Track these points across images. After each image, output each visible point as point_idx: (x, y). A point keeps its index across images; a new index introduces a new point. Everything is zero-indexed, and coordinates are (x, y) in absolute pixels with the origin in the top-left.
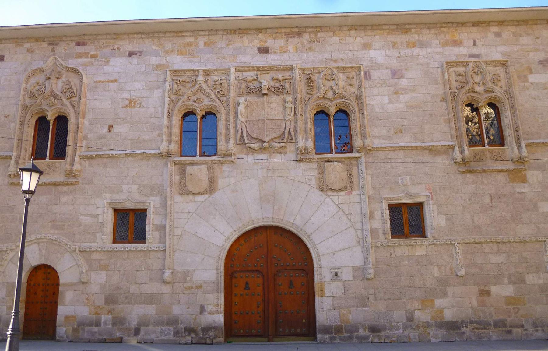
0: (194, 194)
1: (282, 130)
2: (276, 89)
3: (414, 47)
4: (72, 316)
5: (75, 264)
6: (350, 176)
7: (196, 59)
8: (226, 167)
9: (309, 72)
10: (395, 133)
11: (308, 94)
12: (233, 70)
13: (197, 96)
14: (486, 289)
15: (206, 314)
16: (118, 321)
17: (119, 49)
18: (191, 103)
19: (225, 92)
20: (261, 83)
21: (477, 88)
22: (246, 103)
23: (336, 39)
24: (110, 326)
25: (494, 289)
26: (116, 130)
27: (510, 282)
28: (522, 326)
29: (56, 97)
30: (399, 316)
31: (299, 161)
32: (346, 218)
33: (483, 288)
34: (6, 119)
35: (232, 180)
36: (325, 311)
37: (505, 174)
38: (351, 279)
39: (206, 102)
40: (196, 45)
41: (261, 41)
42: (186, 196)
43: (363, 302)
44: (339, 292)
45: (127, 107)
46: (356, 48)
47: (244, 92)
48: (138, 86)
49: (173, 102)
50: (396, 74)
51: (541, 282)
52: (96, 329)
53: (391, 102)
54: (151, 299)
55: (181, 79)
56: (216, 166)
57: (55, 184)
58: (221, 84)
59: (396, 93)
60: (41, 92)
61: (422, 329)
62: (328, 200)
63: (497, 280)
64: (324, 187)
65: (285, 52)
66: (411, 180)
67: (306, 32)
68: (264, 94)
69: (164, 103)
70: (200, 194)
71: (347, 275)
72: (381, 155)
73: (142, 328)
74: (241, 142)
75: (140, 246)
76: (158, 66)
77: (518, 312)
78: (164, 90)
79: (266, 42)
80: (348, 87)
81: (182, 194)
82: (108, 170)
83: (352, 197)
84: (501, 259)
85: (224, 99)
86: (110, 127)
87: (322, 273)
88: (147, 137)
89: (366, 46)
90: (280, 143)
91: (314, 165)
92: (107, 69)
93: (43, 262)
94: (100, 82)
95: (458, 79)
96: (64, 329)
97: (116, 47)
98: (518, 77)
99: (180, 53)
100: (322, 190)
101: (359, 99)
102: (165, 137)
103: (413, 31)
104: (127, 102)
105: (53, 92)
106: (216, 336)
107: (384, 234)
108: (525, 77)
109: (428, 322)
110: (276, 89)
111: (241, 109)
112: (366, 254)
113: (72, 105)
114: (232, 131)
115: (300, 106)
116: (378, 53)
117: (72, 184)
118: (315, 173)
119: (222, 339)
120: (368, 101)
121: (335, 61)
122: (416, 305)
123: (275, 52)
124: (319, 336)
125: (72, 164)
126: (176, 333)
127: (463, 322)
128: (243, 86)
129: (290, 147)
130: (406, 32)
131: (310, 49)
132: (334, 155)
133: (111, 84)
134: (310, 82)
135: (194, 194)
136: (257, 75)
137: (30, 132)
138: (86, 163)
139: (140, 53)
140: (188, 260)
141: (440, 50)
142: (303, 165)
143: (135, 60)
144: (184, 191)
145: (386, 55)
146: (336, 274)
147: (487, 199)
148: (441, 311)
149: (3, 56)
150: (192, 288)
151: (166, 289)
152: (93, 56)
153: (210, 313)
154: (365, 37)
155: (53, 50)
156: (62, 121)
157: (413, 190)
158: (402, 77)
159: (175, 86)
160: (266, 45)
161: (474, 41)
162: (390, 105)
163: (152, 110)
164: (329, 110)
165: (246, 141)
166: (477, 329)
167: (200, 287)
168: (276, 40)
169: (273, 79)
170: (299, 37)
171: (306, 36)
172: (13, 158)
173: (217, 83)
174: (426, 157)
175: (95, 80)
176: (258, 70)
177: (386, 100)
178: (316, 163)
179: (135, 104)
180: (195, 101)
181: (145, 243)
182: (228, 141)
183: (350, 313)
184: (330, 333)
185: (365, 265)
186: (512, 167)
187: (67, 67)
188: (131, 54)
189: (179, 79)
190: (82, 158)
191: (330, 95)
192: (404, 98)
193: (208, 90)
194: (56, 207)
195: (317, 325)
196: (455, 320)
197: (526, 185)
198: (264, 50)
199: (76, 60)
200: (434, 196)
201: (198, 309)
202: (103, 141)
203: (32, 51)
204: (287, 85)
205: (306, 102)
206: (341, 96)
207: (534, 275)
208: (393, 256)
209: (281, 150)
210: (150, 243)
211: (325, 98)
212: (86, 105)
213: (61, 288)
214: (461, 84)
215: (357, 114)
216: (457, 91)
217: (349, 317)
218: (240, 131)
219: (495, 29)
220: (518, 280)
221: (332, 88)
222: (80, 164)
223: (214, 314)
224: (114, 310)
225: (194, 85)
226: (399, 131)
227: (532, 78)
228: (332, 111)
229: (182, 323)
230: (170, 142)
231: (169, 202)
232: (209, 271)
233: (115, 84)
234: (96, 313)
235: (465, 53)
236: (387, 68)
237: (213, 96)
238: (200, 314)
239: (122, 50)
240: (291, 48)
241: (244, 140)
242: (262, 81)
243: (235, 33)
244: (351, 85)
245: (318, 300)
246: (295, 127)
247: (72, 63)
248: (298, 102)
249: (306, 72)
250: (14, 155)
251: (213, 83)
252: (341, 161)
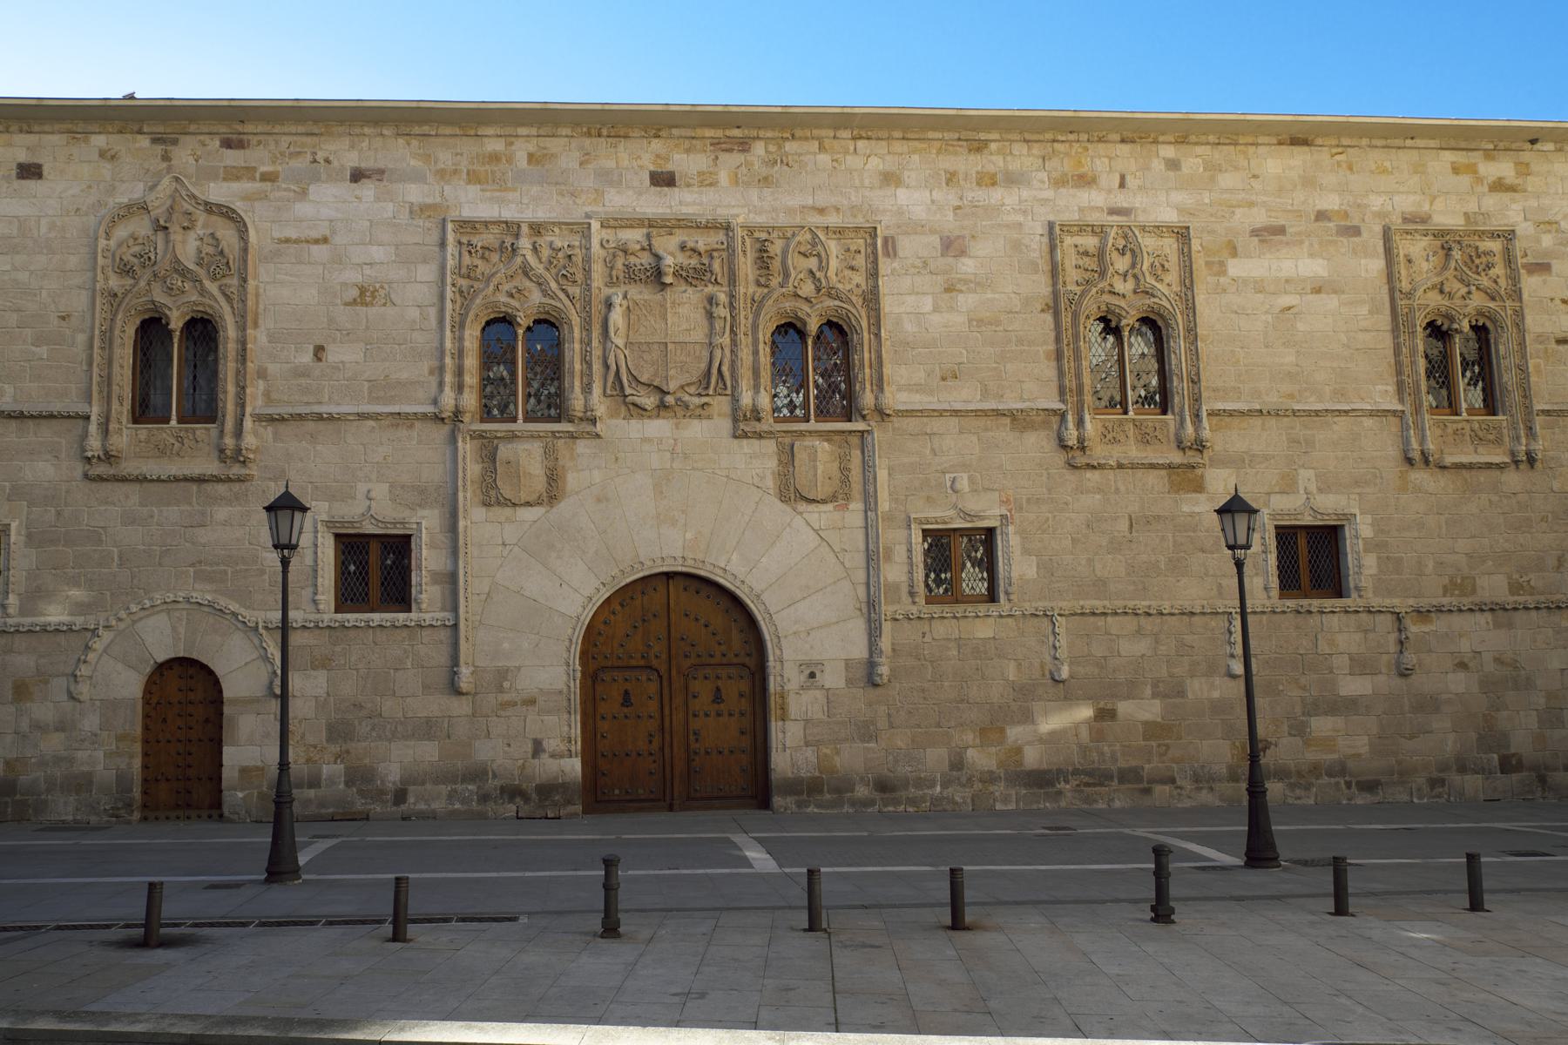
0: (515, 505)
1: (703, 366)
3: (994, 184)
4: (257, 768)
5: (255, 656)
6: (844, 470)
7: (510, 195)
8: (582, 447)
9: (764, 236)
10: (944, 379)
12: (595, 225)
13: (515, 283)
14: (1109, 706)
15: (544, 757)
16: (360, 777)
17: (327, 161)
18: (503, 298)
19: (579, 277)
20: (658, 257)
21: (1120, 286)
22: (625, 303)
23: (824, 159)
24: (342, 786)
25: (1124, 708)
26: (333, 355)
27: (1155, 695)
28: (1173, 781)
29: (184, 273)
30: (935, 758)
32: (834, 560)
33: (1102, 705)
34: (63, 324)
35: (597, 476)
36: (790, 750)
37: (1163, 472)
38: (842, 684)
39: (536, 297)
40: (510, 160)
41: (658, 156)
43: (867, 732)
44: (817, 713)
45: (354, 302)
46: (867, 182)
47: (621, 276)
48: (377, 253)
49: (465, 296)
50: (952, 246)
51: (1216, 694)
52: (312, 793)
53: (936, 309)
54: (427, 729)
55: (478, 241)
56: (560, 443)
57: (201, 480)
59: (947, 290)
60: (146, 260)
61: (978, 786)
62: (798, 521)
63: (1131, 690)
64: (791, 493)
65: (711, 185)
66: (971, 480)
67: (758, 138)
69: (442, 297)
70: (528, 504)
71: (833, 678)
72: (911, 424)
73: (411, 788)
74: (617, 390)
75: (401, 617)
76: (424, 208)
77: (1165, 754)
78: (443, 268)
79: (667, 159)
80: (848, 273)
81: (486, 504)
82: (319, 447)
83: (847, 514)
84: (1142, 647)
85: (575, 291)
86: (319, 351)
87: (784, 673)
88: (404, 375)
89: (890, 179)
90: (700, 395)
91: (770, 446)
92: (303, 209)
93: (181, 655)
94: (287, 241)
95: (1081, 263)
96: (240, 795)
97: (320, 156)
98: (1207, 263)
99: (473, 178)
100: (784, 498)
101: (872, 299)
102: (448, 378)
103: (993, 146)
104: (355, 293)
105: (178, 261)
106: (569, 802)
107: (912, 594)
108: (1222, 264)
109: (992, 772)
111: (617, 317)
112: (873, 633)
113: (224, 294)
114: (597, 367)
115: (743, 313)
116: (914, 198)
117: (240, 480)
118: (772, 464)
119: (579, 808)
120: (888, 305)
121: (822, 211)
122: (969, 737)
123: (688, 185)
124: (777, 801)
125: (239, 432)
126: (484, 798)
127: (1059, 771)
128: (619, 264)
129: (721, 404)
130: (978, 150)
131: (766, 181)
132: (813, 425)
133: (315, 248)
134: (763, 260)
135: (515, 505)
136: (649, 236)
137: (125, 355)
138: (268, 432)
139: (380, 174)
140: (506, 645)
141: (1049, 194)
142: (749, 446)
143: (367, 190)
144: (492, 498)
145: (933, 202)
146: (812, 675)
147: (1124, 525)
148: (1019, 750)
149: (39, 166)
150: (515, 704)
151: (460, 707)
152: (266, 177)
153: (552, 756)
154: (888, 158)
155: (166, 158)
156: (202, 330)
157: (972, 505)
158: (963, 253)
159: (467, 260)
160: (670, 167)
161: (1123, 178)
162: (936, 318)
163: (414, 313)
164: (805, 324)
165: (628, 391)
166: (1088, 785)
167: (531, 702)
168: (692, 156)
169: (683, 248)
170: (743, 151)
171: (759, 149)
172: (94, 418)
173: (560, 255)
174: (1003, 433)
175: (276, 235)
176: (650, 226)
177: (927, 304)
178: (773, 442)
179: (374, 297)
180: (512, 296)
181: (410, 611)
182: (587, 389)
183: (838, 753)
184: (800, 793)
185: (871, 656)
186: (1176, 457)
187: (206, 203)
188: (357, 176)
189: (474, 241)
190: (258, 418)
191: (808, 289)
192: (967, 301)
193: (539, 269)
194: (202, 531)
195: (773, 776)
196: (1045, 766)
197: (1202, 497)
198: (664, 180)
199: (225, 184)
200: (1016, 516)
201: (529, 747)
202: (303, 381)
203: (113, 157)
205: (757, 305)
206: (832, 293)
207: (1203, 680)
208: (928, 639)
209: (703, 411)
210: (420, 610)
211: (796, 295)
212: (257, 295)
213: (227, 710)
214: (1087, 275)
215: (866, 334)
216: (1078, 290)
217: (837, 761)
218: (613, 367)
219: (1168, 152)
220: (1171, 691)
221: (811, 272)
222: (256, 434)
223: (562, 757)
224: (348, 752)
226: (951, 376)
227: (1236, 268)
228: (813, 326)
229: (495, 776)
230: (460, 388)
231: (461, 524)
232: (551, 670)
233: (324, 247)
234: (308, 761)
235: (1101, 204)
236: (932, 231)
237: (553, 285)
238: (534, 757)
239: (335, 163)
240: (723, 177)
241: (622, 388)
242: (661, 252)
243: (600, 136)
244: (852, 268)
245: (775, 726)
246: (733, 362)
247: (217, 192)
248: (740, 304)
249: (756, 235)
250: (95, 411)
252: (827, 436)
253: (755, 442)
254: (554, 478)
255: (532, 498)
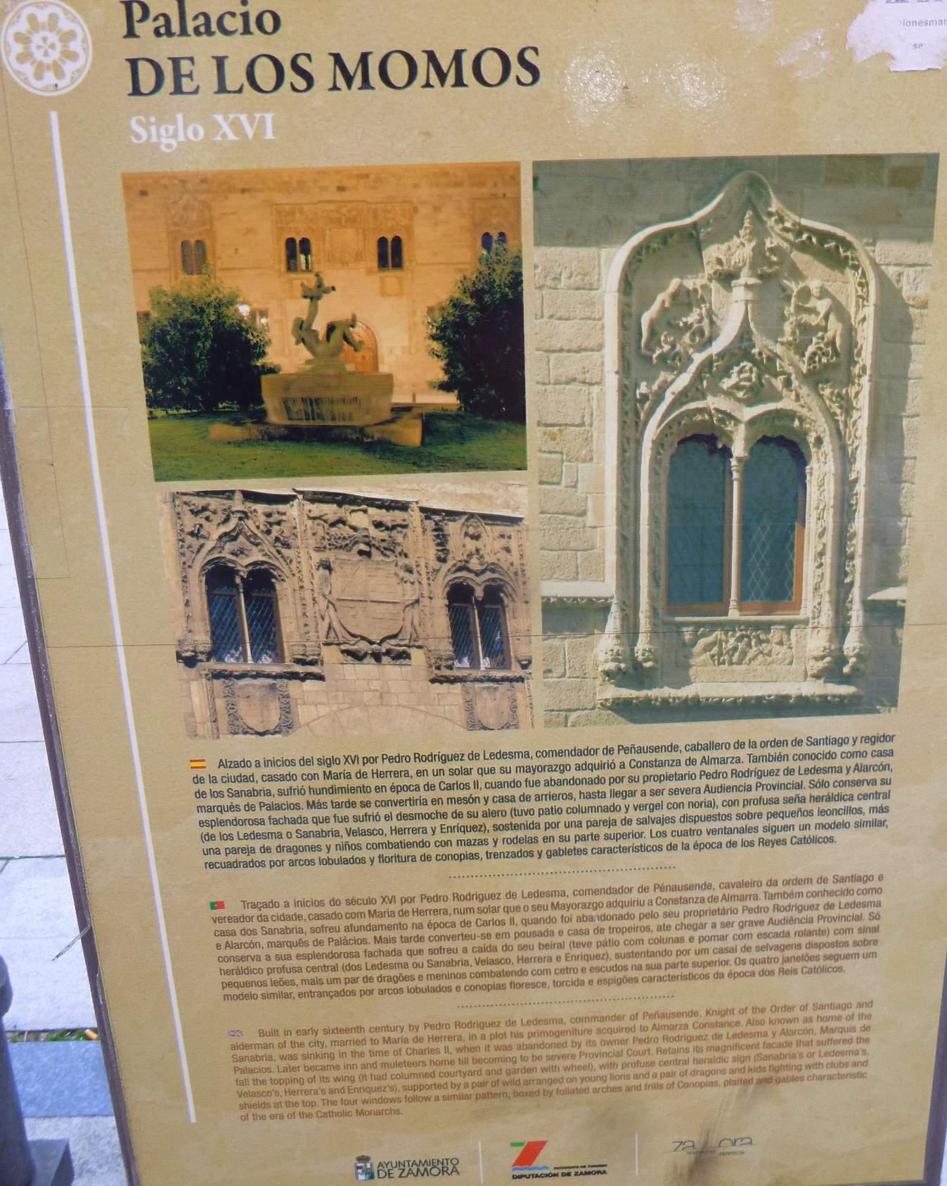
2: (383, 544)
8: (309, 685)
11: (439, 559)
19: (290, 541)
31: (433, 681)
39: (256, 556)
42: (241, 736)
47: (326, 543)
58: (279, 523)
68: (361, 553)
110: (383, 544)
134: (441, 539)
204: (399, 539)
205: (436, 571)
225: (227, 520)
228: (479, 593)
251: (262, 519)
253: (445, 685)
254: (287, 710)
255: (272, 727)
